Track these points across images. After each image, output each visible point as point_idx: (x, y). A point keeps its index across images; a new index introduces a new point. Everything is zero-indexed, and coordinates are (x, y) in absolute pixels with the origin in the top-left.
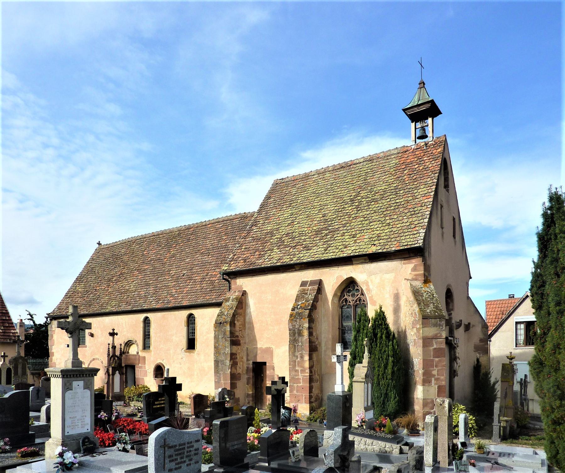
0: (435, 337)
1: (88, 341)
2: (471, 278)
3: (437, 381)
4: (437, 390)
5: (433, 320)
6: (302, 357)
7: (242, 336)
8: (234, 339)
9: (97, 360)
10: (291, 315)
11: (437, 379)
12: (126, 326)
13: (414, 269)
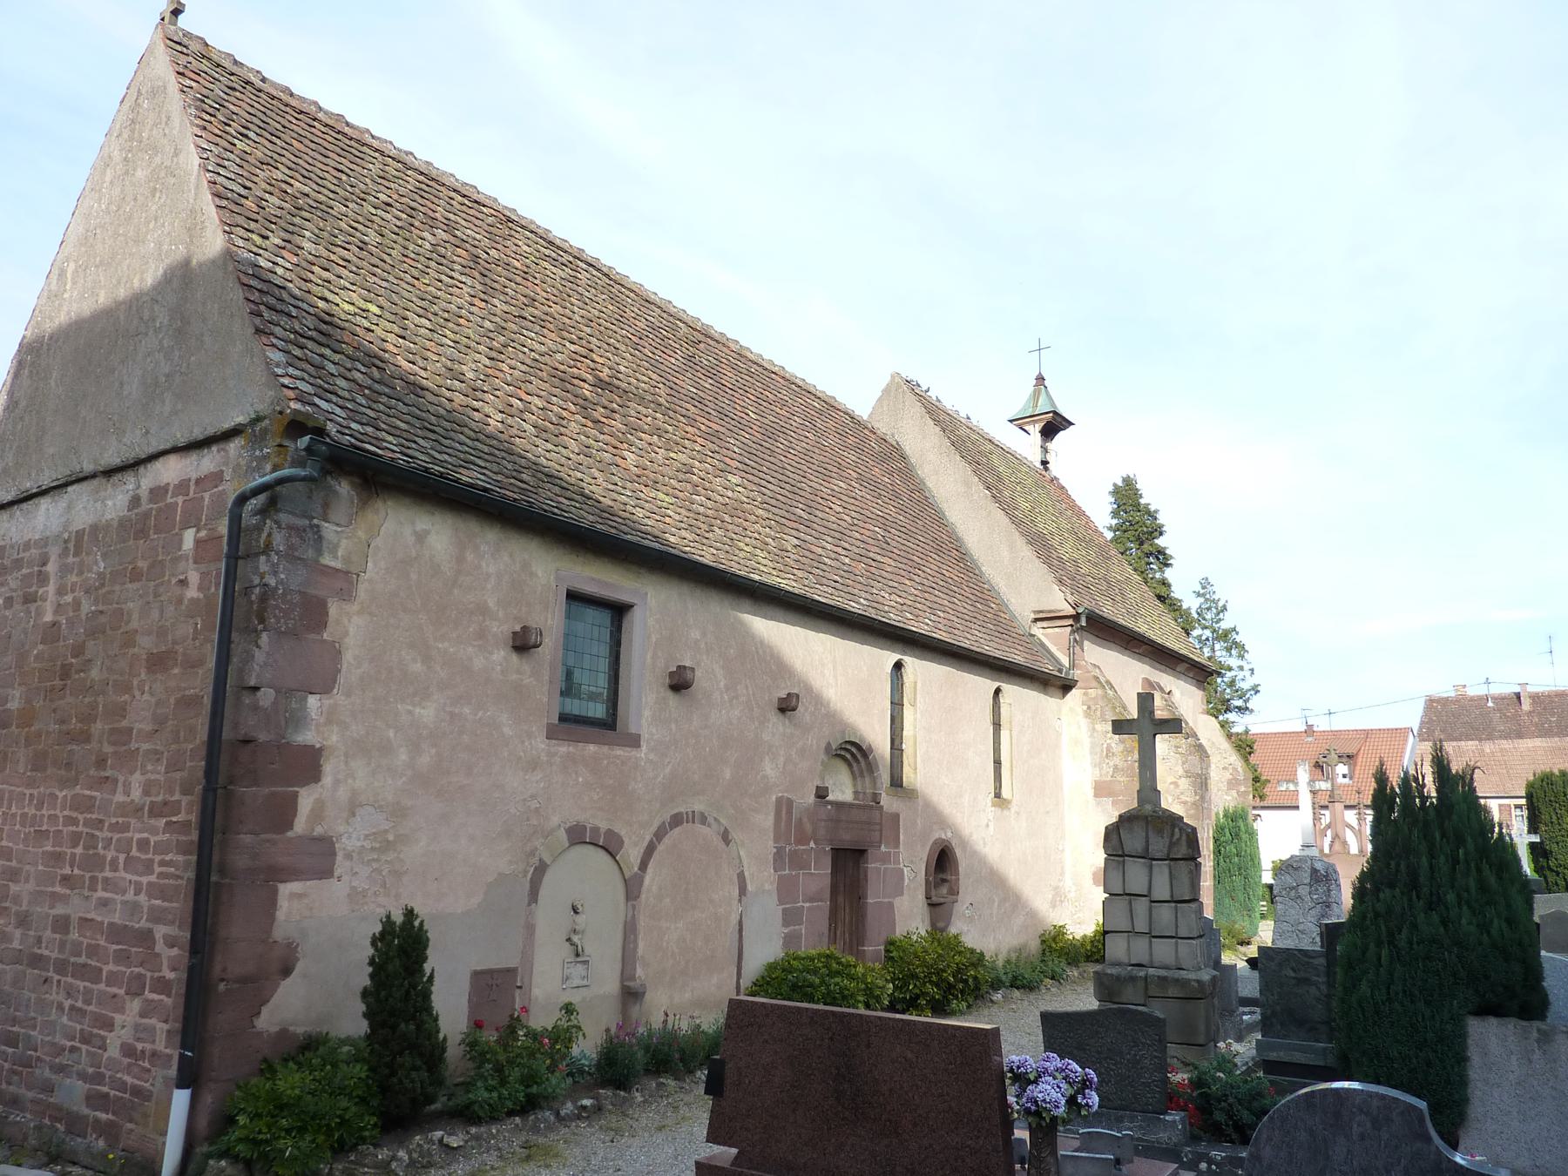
1: (647, 713)
9: (698, 826)
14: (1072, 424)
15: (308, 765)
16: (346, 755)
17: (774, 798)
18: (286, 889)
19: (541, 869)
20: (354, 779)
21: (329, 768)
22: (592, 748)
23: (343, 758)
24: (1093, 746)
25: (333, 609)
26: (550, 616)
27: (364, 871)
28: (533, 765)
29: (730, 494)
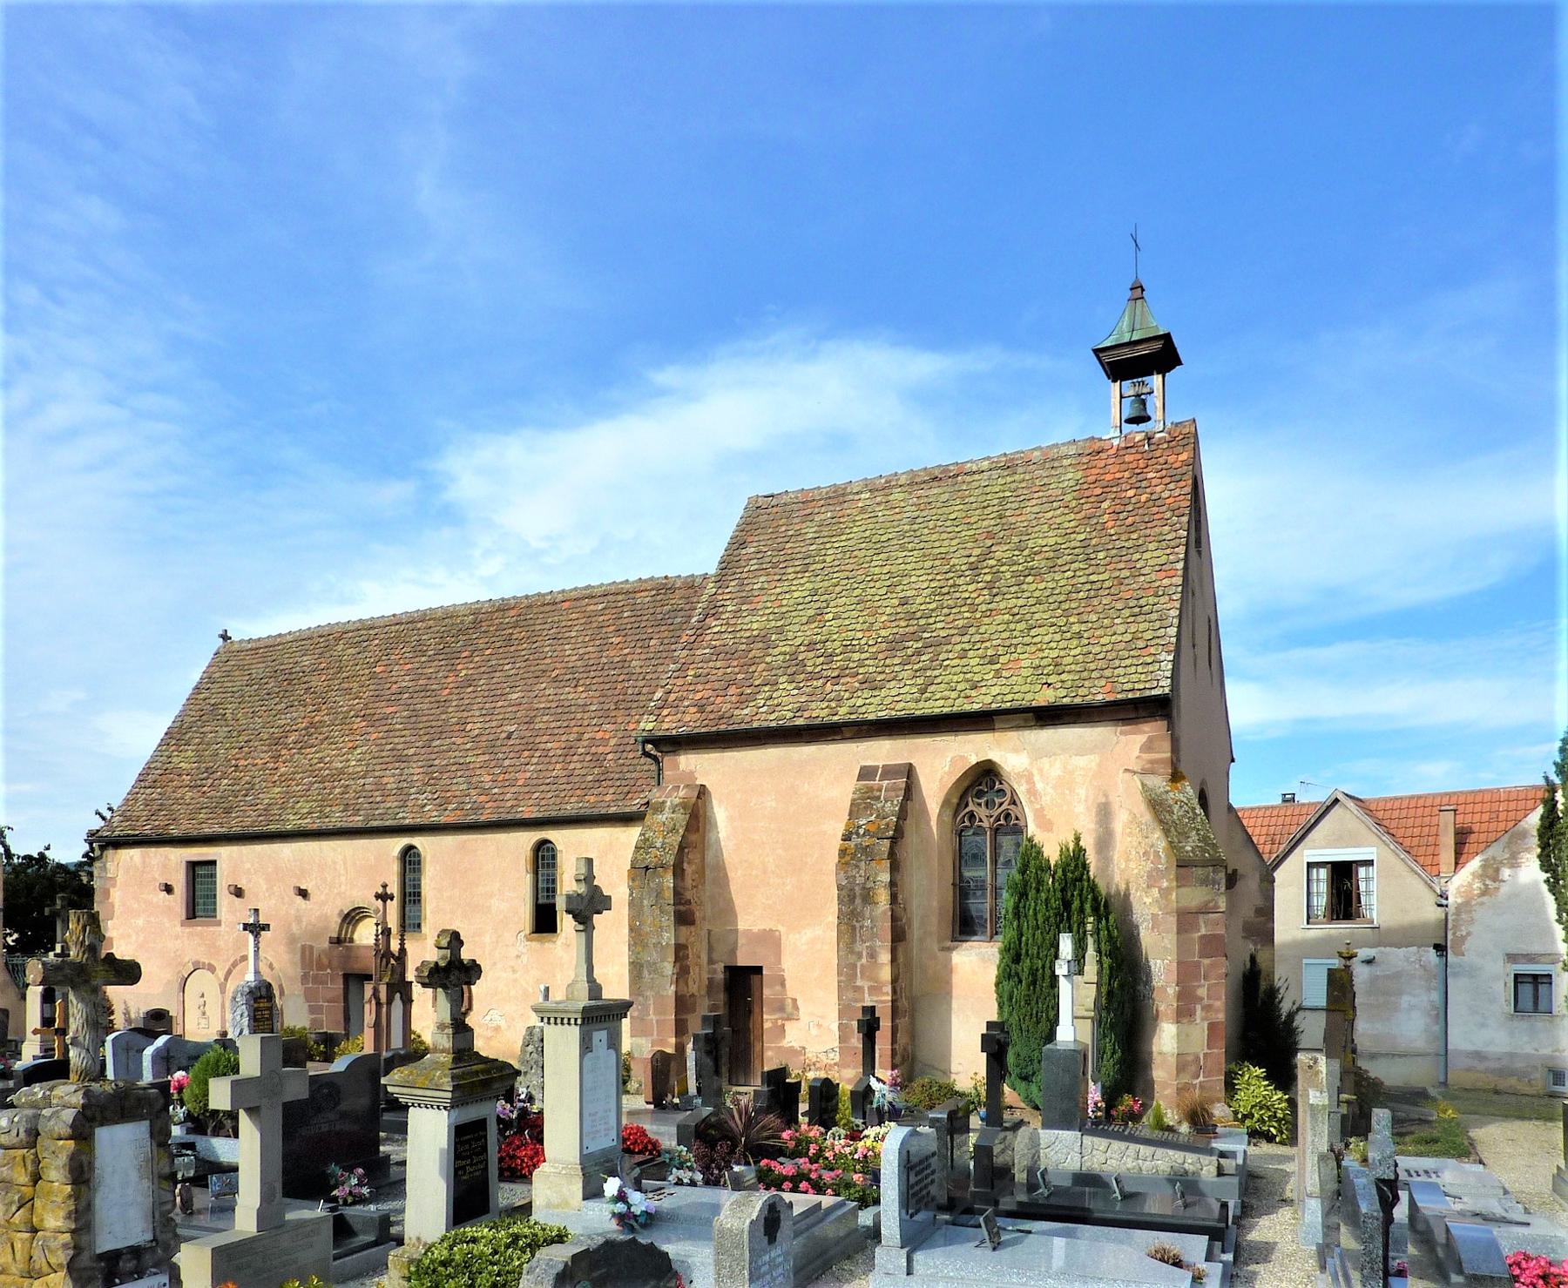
0: (1204, 910)
1: (224, 909)
2: (1233, 760)
3: (1208, 1011)
4: (1206, 1032)
5: (1200, 871)
6: (873, 955)
7: (699, 902)
8: (682, 908)
10: (841, 850)
11: (1207, 1008)
12: (346, 869)
13: (1147, 747)
17: (299, 945)
25: (111, 890)
28: (177, 937)
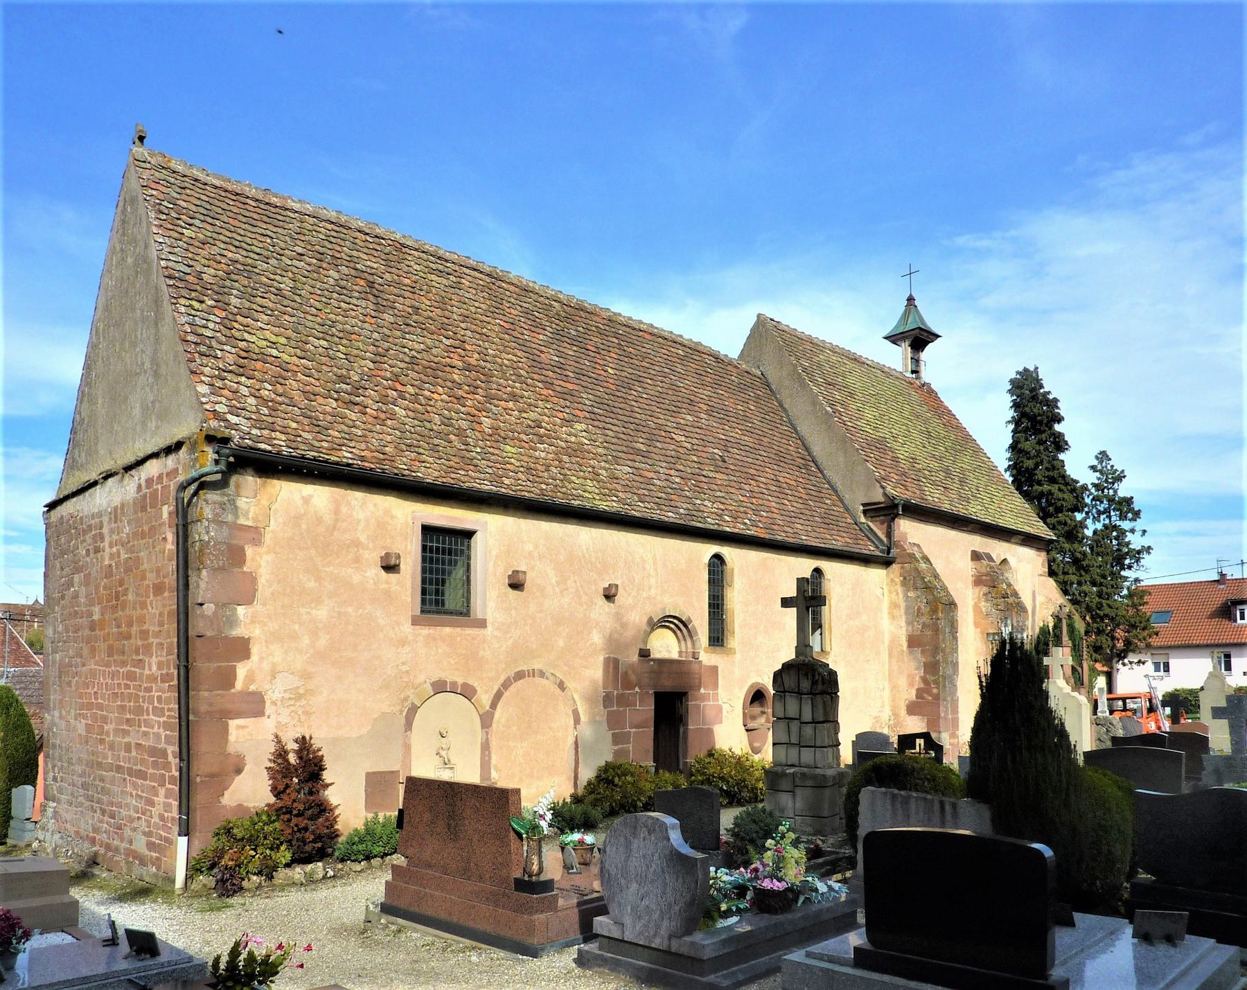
9: (537, 680)
12: (656, 570)
14: (940, 336)
15: (241, 649)
16: (266, 642)
18: (233, 724)
19: (413, 710)
20: (274, 656)
21: (255, 649)
22: (448, 630)
23: (264, 644)
24: (907, 608)
26: (409, 544)
27: (285, 712)
28: (403, 642)
29: (573, 439)
